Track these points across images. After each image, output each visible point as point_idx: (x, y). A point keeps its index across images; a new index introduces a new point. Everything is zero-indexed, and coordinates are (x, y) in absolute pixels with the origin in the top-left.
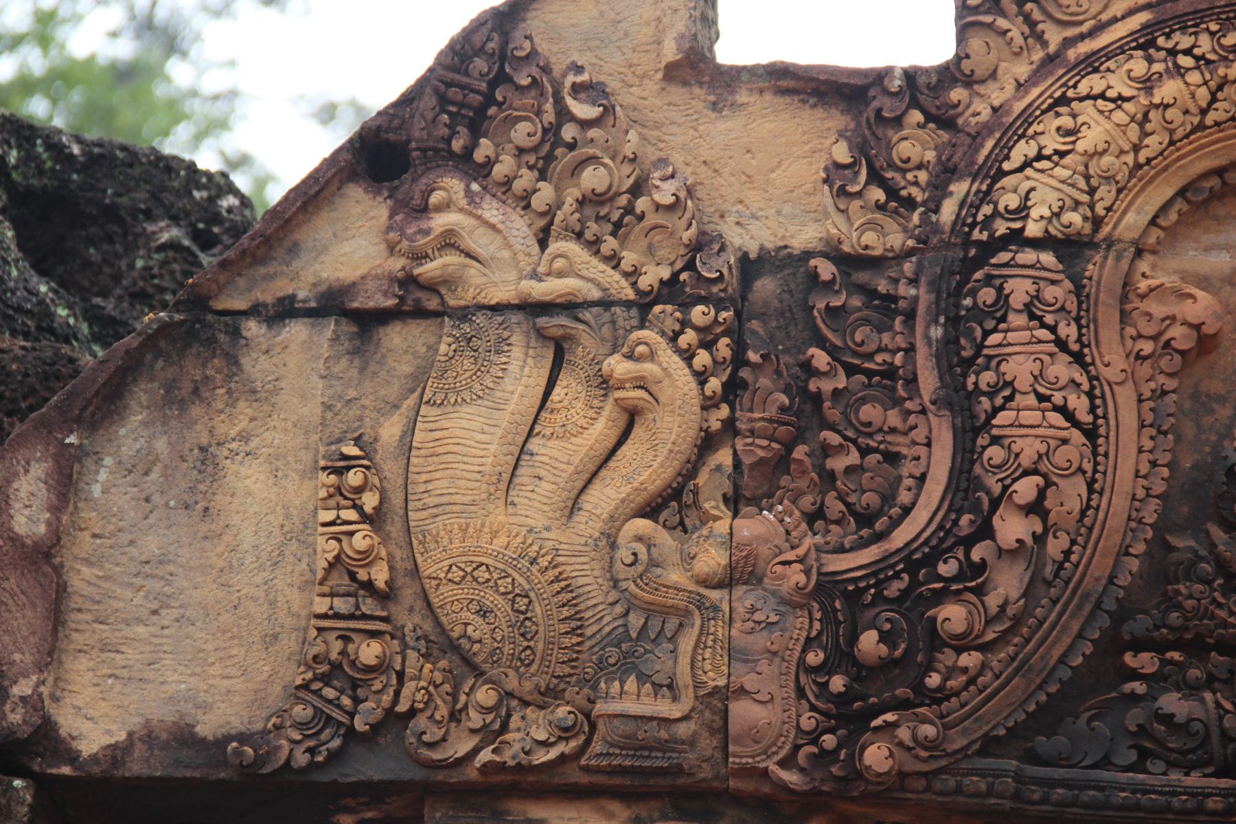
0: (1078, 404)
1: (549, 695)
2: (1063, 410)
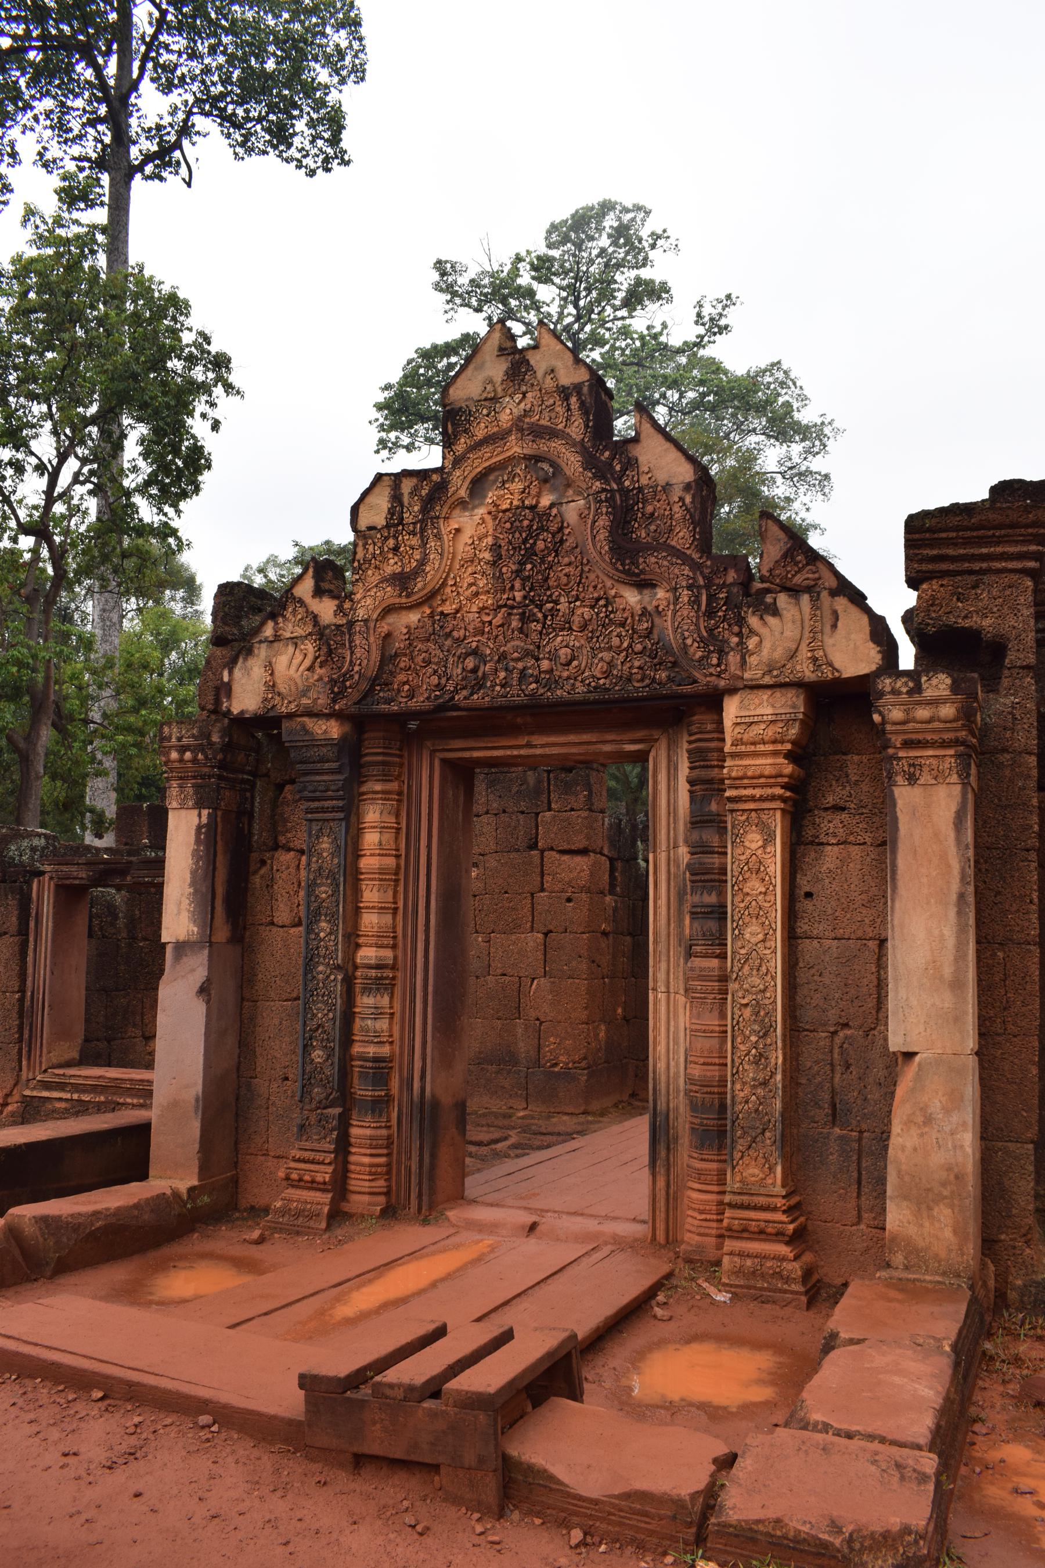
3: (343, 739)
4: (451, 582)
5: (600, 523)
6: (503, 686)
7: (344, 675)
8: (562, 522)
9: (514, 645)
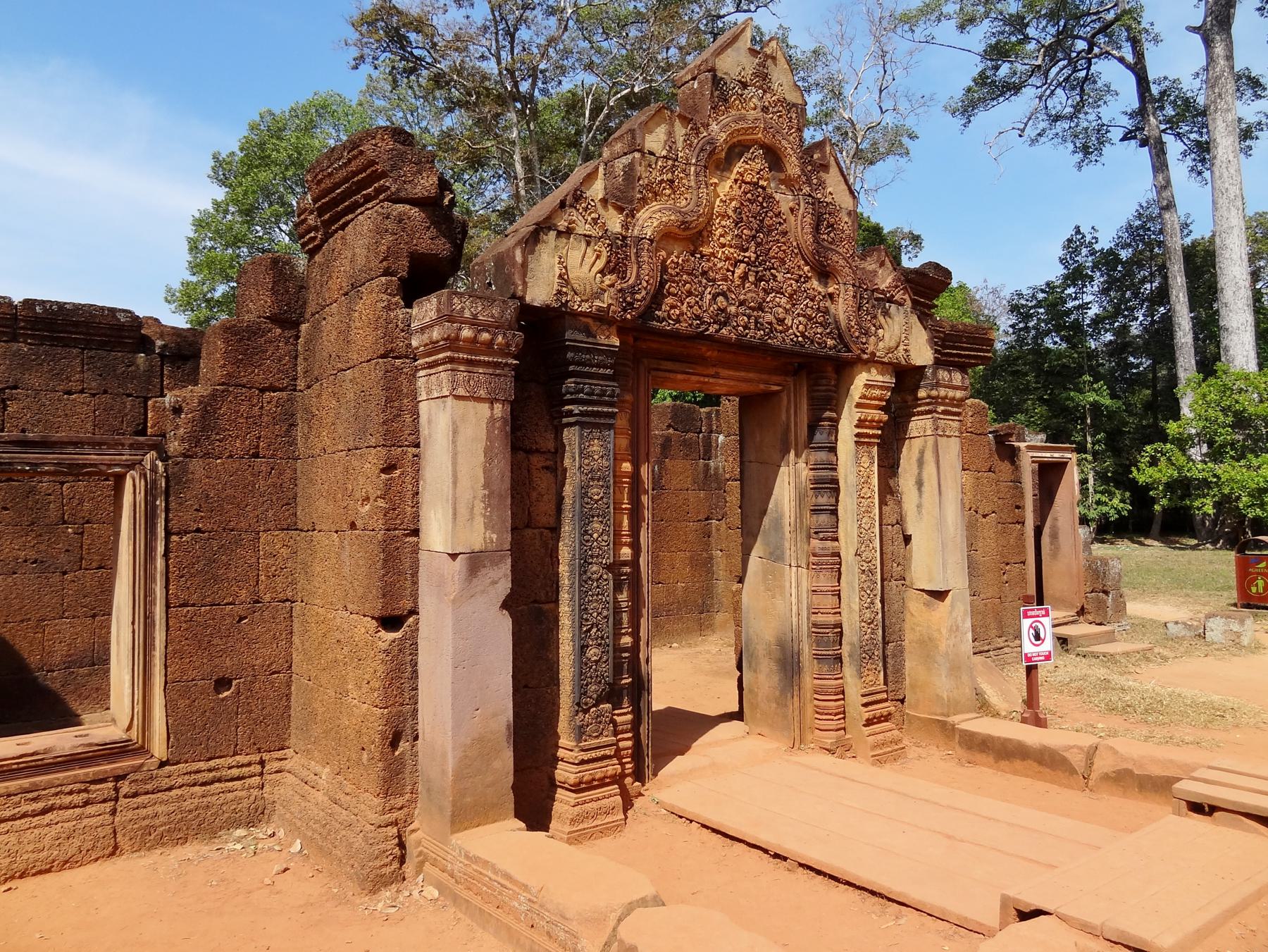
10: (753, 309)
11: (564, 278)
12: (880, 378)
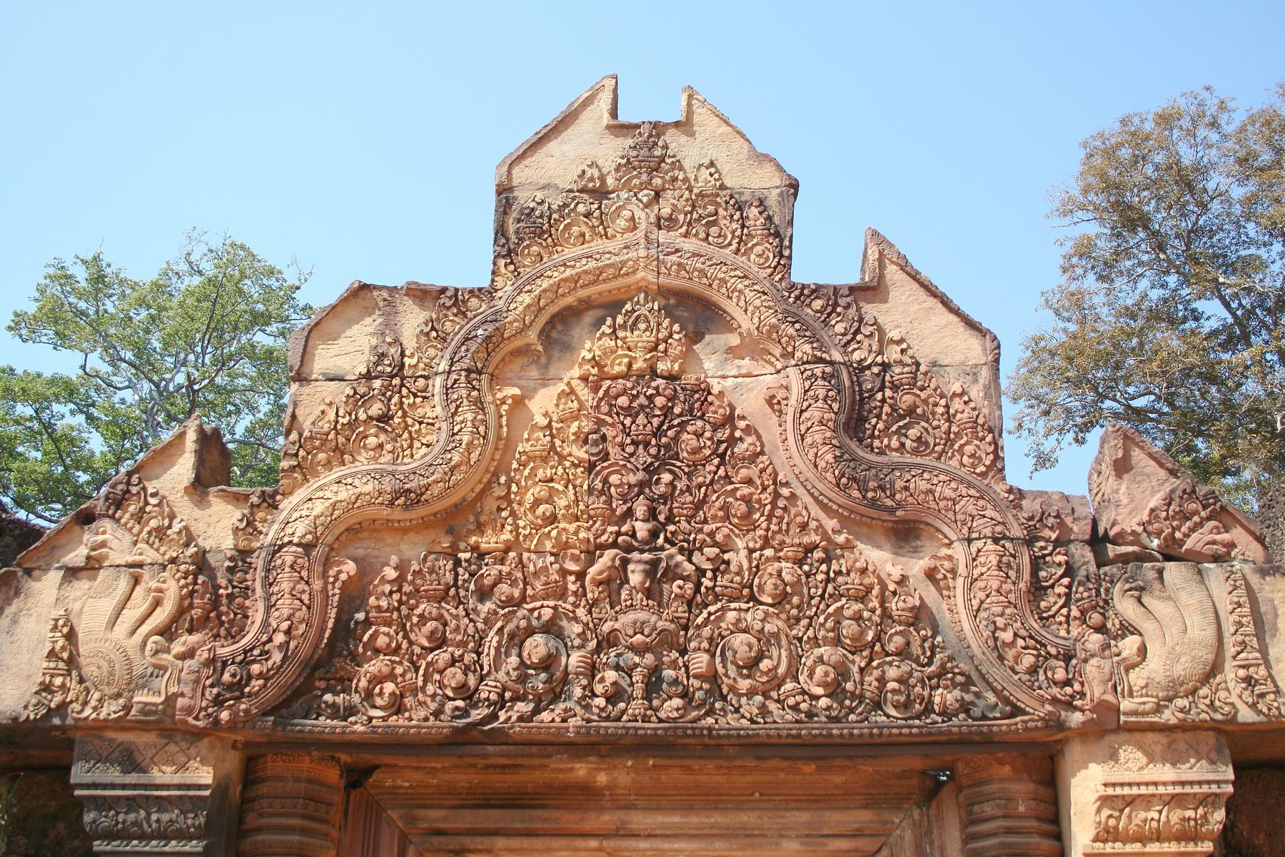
0: (305, 597)
1: (119, 695)
2: (302, 601)
3: (220, 788)
4: (499, 492)
5: (814, 413)
6: (612, 699)
7: (245, 652)
8: (733, 409)
9: (632, 619)
10: (640, 650)
11: (67, 654)
12: (1165, 772)
